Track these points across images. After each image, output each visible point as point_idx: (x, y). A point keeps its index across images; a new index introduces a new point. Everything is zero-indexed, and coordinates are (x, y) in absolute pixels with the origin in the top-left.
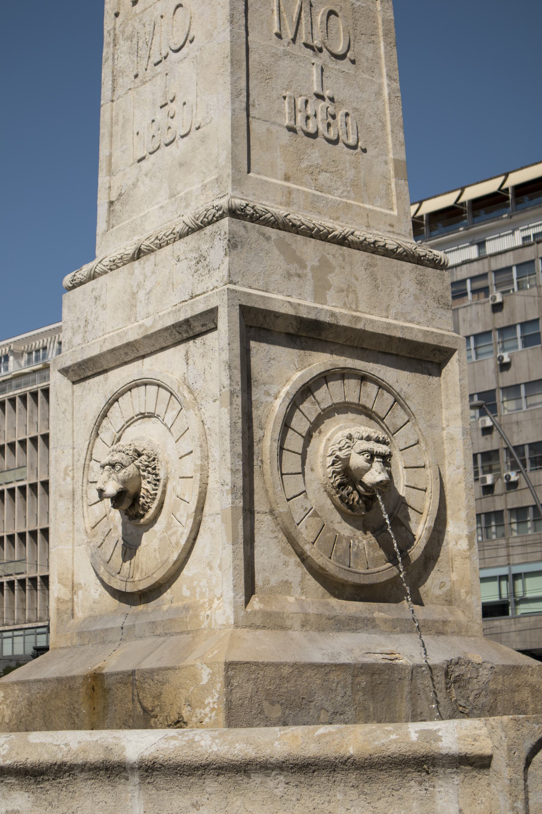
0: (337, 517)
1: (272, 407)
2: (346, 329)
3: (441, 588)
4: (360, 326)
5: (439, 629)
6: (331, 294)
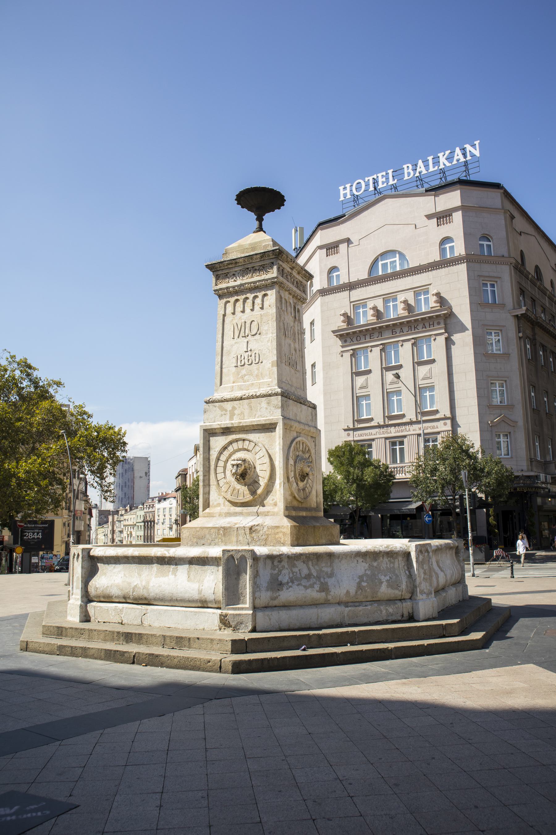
0: (236, 483)
1: (214, 454)
2: (237, 427)
3: (272, 500)
4: (241, 425)
5: (266, 514)
6: (235, 417)
